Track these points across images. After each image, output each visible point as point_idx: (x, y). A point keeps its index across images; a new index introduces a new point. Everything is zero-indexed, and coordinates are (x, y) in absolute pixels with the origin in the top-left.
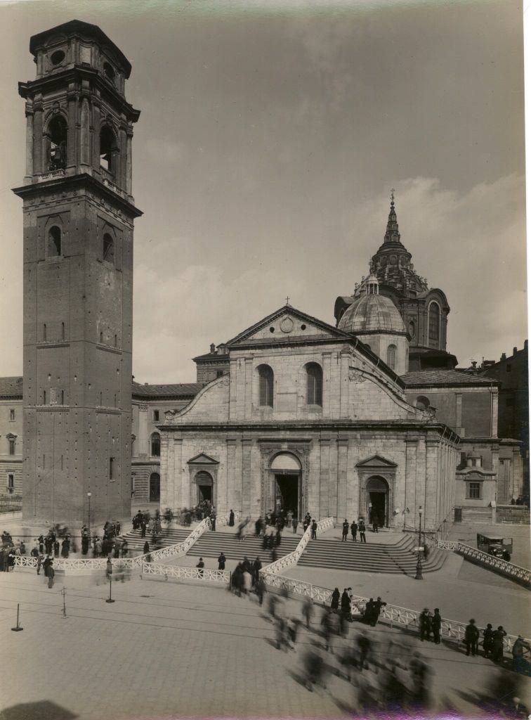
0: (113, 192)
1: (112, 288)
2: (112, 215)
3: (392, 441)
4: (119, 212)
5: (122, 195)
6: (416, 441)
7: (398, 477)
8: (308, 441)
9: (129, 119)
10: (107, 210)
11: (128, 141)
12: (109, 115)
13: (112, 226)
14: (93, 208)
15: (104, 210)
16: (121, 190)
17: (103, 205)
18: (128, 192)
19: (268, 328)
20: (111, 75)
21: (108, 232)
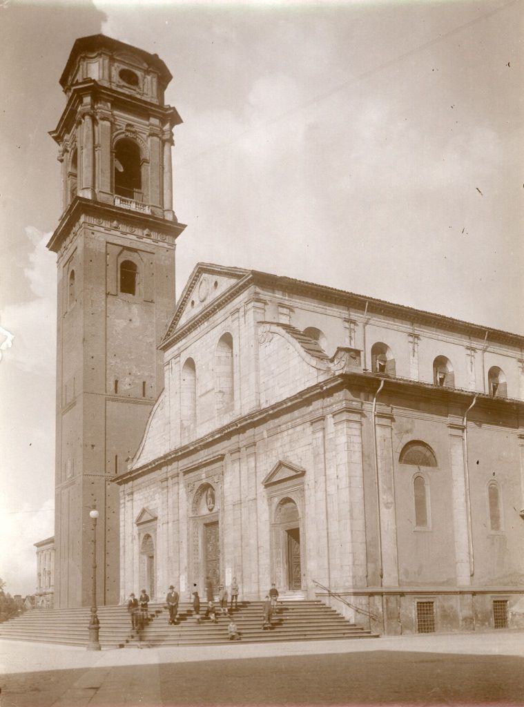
0: (129, 211)
1: (137, 323)
2: (134, 237)
3: (299, 428)
4: (146, 232)
5: (147, 211)
6: (323, 418)
7: (307, 493)
8: (222, 458)
9: (163, 122)
10: (123, 233)
11: (166, 148)
12: (128, 125)
13: (135, 250)
14: (99, 234)
15: (118, 234)
16: (144, 206)
17: (116, 228)
18: (166, 206)
19: (189, 304)
20: (129, 77)
21: (130, 258)
